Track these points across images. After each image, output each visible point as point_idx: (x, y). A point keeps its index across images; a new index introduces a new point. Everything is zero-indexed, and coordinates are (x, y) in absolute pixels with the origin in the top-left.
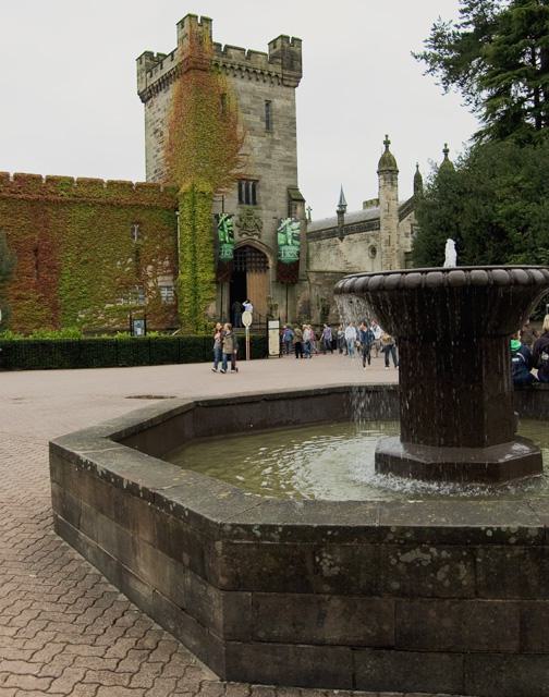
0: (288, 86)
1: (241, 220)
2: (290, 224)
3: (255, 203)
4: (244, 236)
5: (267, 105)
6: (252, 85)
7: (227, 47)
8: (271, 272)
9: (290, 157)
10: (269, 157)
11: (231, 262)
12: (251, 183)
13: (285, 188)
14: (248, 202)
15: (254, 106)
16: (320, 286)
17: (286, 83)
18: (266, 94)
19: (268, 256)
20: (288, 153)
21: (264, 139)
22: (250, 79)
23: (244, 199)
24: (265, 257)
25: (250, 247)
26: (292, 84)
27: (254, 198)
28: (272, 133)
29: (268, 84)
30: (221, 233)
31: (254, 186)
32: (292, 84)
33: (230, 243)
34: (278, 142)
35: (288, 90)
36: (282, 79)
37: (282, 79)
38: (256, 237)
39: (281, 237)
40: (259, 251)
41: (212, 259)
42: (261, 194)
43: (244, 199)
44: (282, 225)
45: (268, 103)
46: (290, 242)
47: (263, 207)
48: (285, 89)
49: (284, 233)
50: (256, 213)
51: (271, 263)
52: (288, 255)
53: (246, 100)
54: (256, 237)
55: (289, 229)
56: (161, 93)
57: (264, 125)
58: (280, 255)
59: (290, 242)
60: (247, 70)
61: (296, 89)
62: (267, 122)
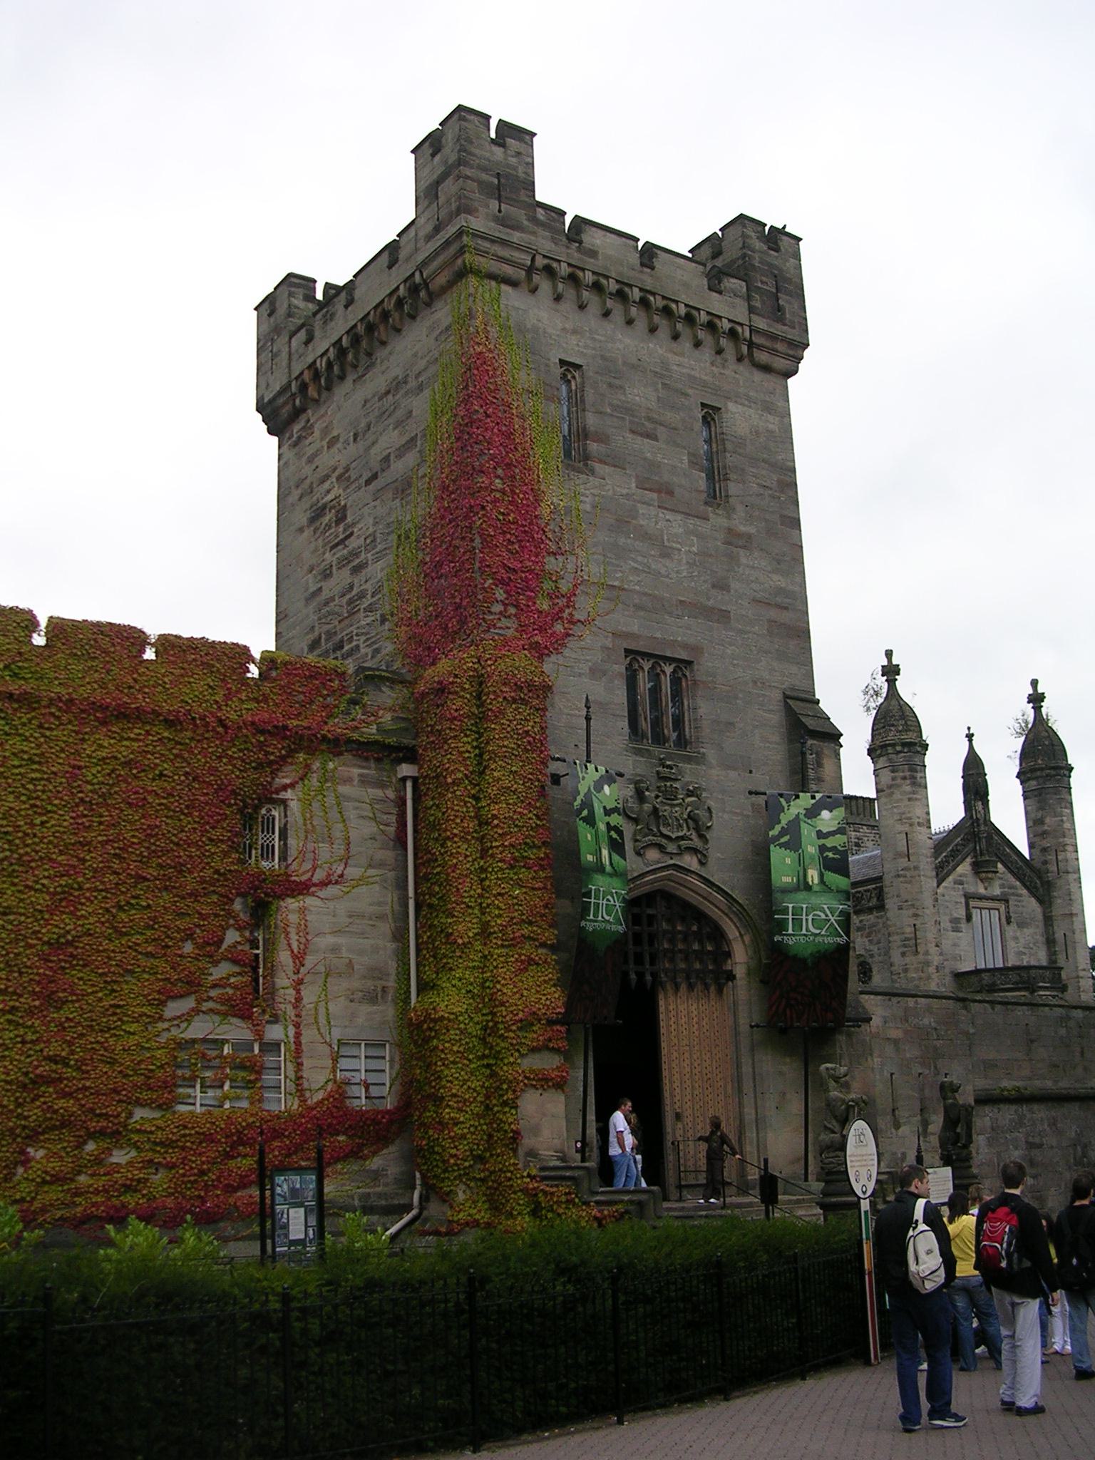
0: (766, 369)
1: (640, 796)
2: (812, 813)
3: (682, 742)
4: (653, 854)
5: (707, 421)
6: (657, 349)
7: (580, 222)
8: (743, 989)
9: (780, 591)
10: (721, 586)
11: (619, 943)
12: (669, 669)
13: (777, 695)
14: (659, 739)
15: (669, 416)
16: (896, 1042)
17: (762, 357)
18: (705, 385)
19: (731, 931)
20: (779, 581)
21: (704, 527)
22: (653, 330)
23: (645, 725)
24: (718, 935)
25: (668, 896)
26: (780, 363)
27: (678, 723)
28: (730, 511)
29: (707, 353)
30: (586, 834)
31: (676, 681)
32: (780, 363)
33: (616, 873)
34: (746, 542)
35: (768, 381)
36: (751, 345)
37: (751, 345)
38: (690, 861)
39: (783, 865)
40: (700, 916)
41: (550, 936)
42: (704, 709)
43: (645, 725)
44: (785, 819)
45: (710, 415)
46: (813, 875)
47: (710, 753)
48: (758, 376)
49: (794, 844)
50: (689, 774)
51: (741, 957)
52: (809, 927)
53: (640, 394)
54: (690, 861)
55: (807, 831)
56: (341, 390)
57: (701, 481)
58: (782, 925)
59: (813, 875)
60: (644, 303)
61: (791, 381)
62: (711, 477)
